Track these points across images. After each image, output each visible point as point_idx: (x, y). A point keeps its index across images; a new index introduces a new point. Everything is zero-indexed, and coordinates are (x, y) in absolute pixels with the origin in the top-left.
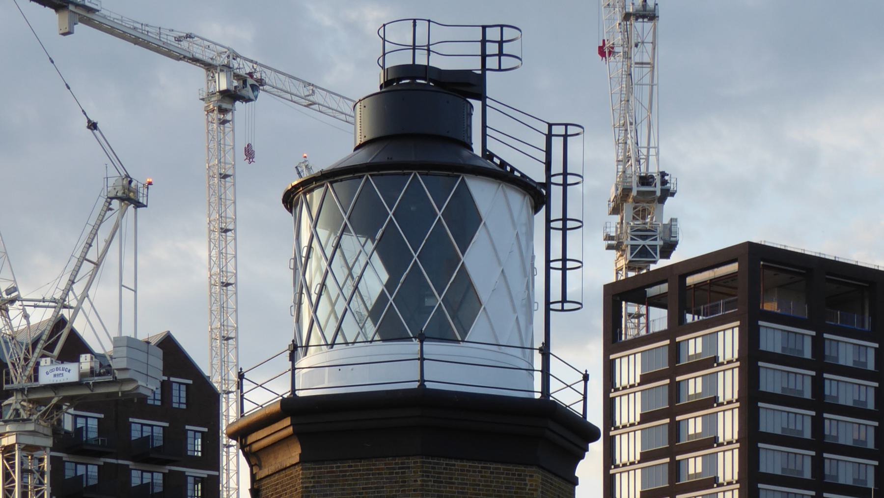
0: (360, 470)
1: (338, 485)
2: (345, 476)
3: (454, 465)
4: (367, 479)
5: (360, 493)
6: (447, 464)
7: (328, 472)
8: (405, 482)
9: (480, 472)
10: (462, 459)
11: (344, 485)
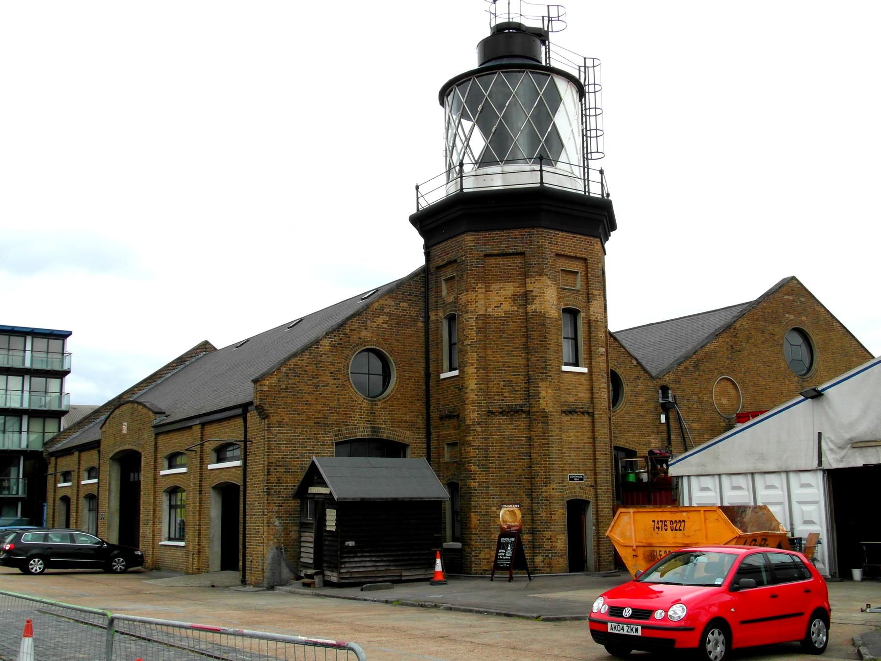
0: (503, 236)
1: (489, 245)
2: (494, 239)
3: (558, 234)
4: (507, 241)
5: (504, 250)
6: (555, 233)
7: (483, 237)
8: (531, 243)
9: (572, 239)
10: (562, 231)
11: (493, 245)
